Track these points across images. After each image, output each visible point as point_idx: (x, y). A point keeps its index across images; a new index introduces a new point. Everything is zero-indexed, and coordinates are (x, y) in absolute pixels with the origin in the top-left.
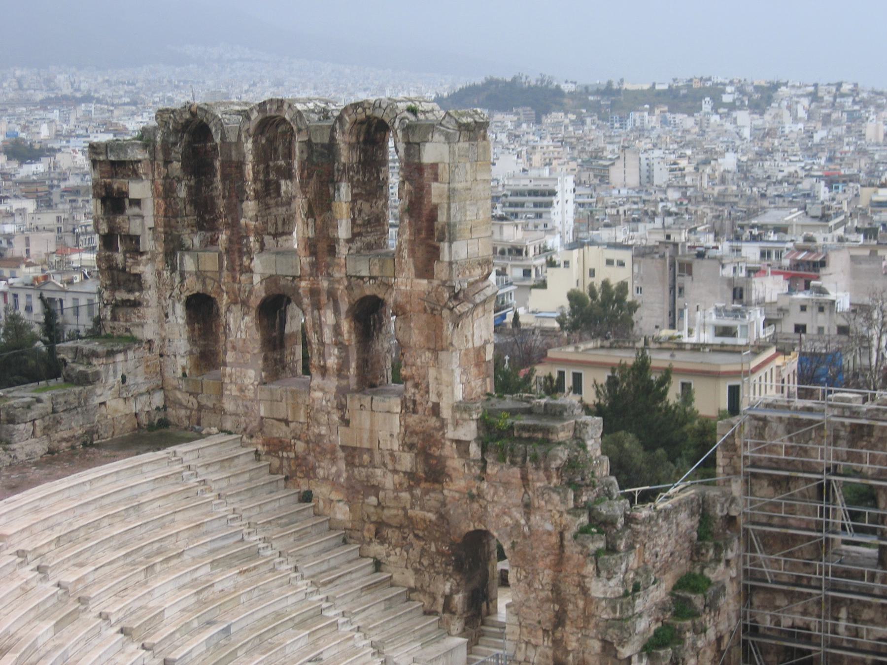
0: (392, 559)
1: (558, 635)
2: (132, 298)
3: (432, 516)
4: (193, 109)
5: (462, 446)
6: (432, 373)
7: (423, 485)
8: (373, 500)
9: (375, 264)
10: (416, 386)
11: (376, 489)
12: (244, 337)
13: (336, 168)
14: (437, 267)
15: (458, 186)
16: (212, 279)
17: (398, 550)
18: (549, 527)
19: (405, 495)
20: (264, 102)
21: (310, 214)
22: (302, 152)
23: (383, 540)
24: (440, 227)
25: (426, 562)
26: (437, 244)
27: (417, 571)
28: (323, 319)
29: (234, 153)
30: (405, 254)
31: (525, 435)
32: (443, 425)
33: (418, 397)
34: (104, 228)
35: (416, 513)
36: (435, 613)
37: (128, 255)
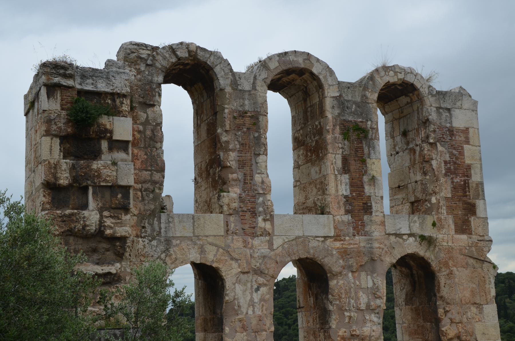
2: (114, 271)
4: (192, 48)
9: (415, 222)
12: (258, 312)
13: (369, 126)
16: (216, 246)
20: (286, 53)
21: (346, 169)
22: (333, 107)
24: (474, 185)
26: (474, 201)
28: (358, 283)
29: (247, 102)
30: (444, 210)
34: (64, 179)
37: (106, 213)
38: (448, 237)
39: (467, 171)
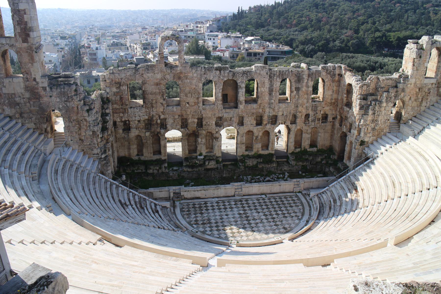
0: (27, 121)
1: (79, 132)
3: (38, 108)
5: (44, 89)
6: (32, 70)
7: (33, 100)
8: (18, 107)
10: (27, 74)
11: (18, 104)
14: (29, 39)
15: (32, 16)
17: (28, 119)
18: (73, 106)
19: (28, 104)
23: (22, 117)
25: (38, 121)
27: (35, 124)
31: (62, 83)
32: (38, 83)
33: (28, 77)
35: (32, 108)
36: (43, 133)
38: (20, 44)
39: (26, 23)
